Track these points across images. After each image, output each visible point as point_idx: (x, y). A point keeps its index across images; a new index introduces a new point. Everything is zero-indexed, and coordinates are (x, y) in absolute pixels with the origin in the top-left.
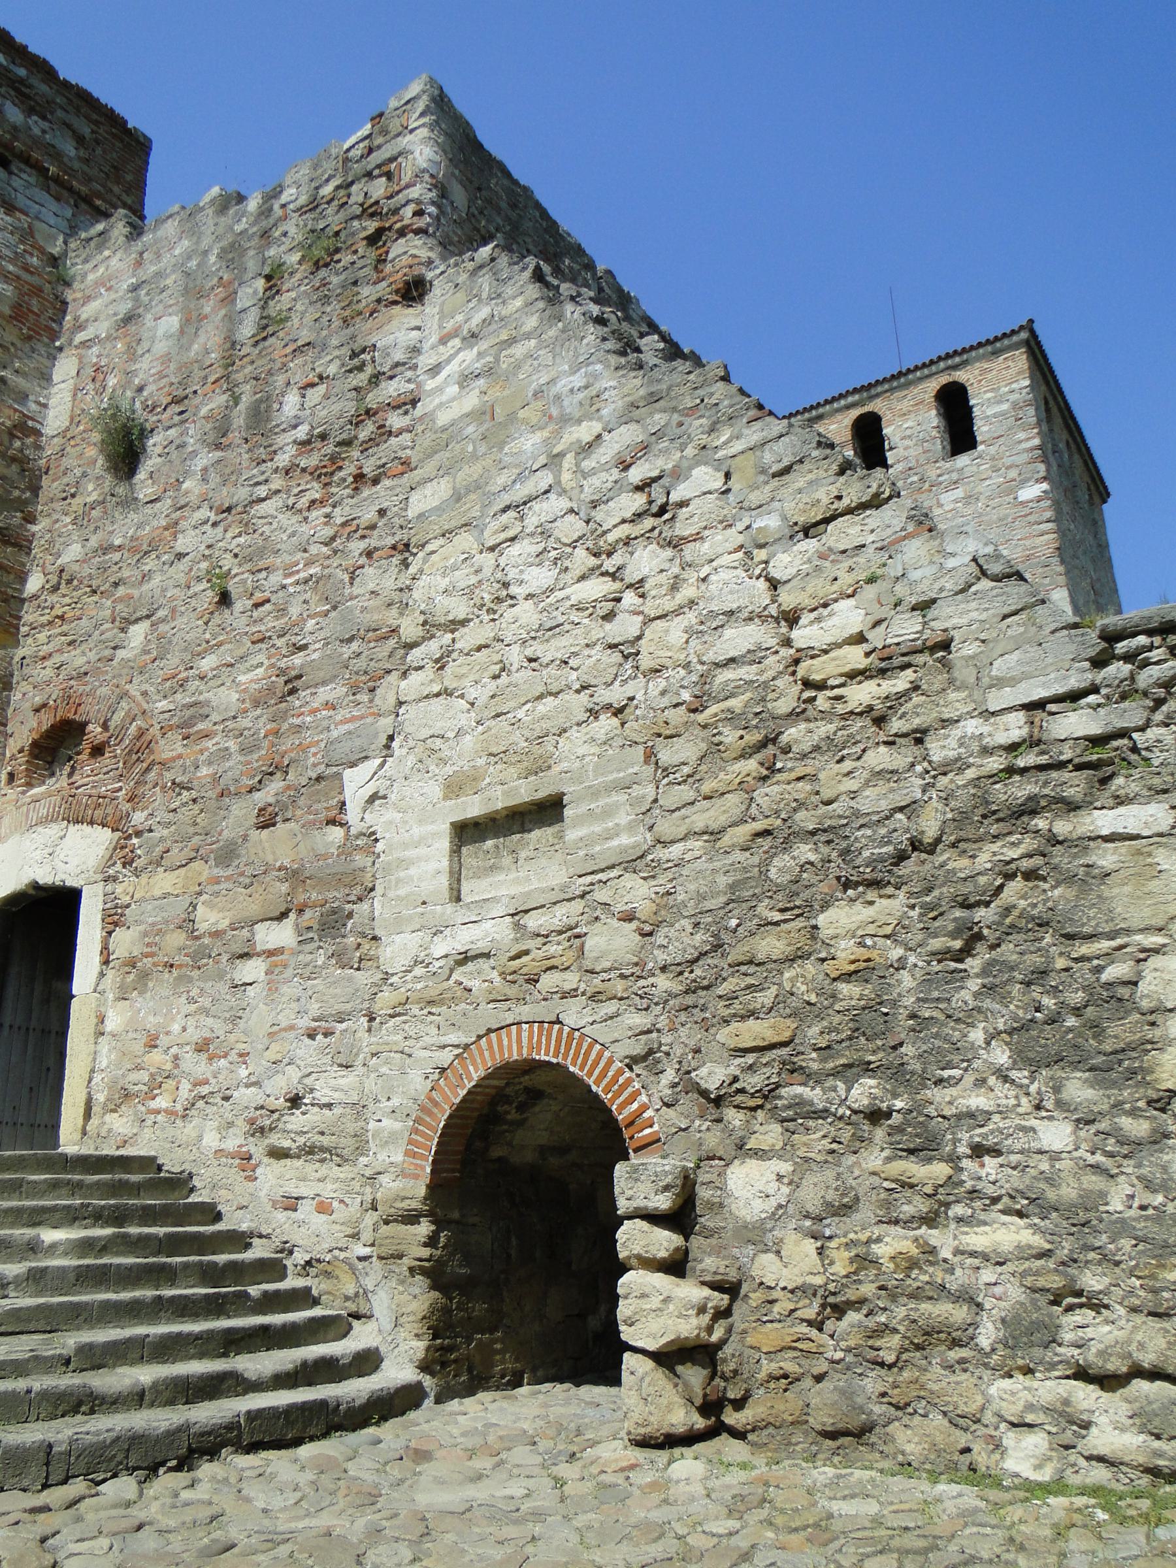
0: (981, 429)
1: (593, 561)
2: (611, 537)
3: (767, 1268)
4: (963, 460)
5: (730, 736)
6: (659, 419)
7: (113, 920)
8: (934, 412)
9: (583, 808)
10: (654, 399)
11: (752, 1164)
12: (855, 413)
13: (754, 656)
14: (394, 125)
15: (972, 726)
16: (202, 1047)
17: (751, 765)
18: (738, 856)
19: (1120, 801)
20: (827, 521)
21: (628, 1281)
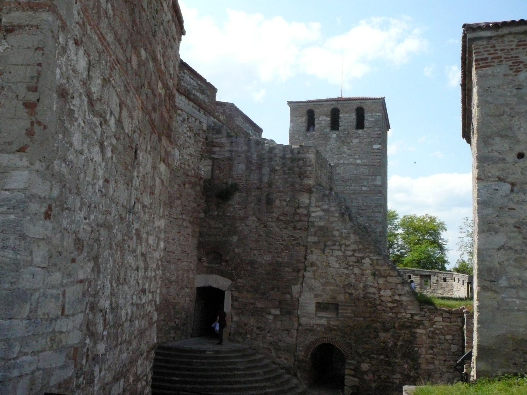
0: (366, 124)
1: (346, 266)
2: (351, 263)
3: (365, 377)
4: (360, 131)
5: (369, 304)
6: (361, 247)
7: (234, 299)
8: (354, 114)
9: (342, 308)
10: (360, 242)
11: (365, 364)
12: (333, 107)
13: (374, 294)
14: (306, 150)
15: (404, 314)
16: (259, 328)
17: (372, 310)
18: (368, 322)
19: (420, 329)
20: (388, 276)
21: (346, 377)
